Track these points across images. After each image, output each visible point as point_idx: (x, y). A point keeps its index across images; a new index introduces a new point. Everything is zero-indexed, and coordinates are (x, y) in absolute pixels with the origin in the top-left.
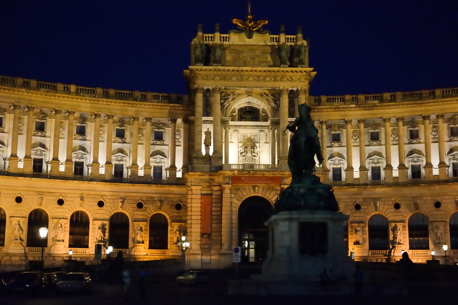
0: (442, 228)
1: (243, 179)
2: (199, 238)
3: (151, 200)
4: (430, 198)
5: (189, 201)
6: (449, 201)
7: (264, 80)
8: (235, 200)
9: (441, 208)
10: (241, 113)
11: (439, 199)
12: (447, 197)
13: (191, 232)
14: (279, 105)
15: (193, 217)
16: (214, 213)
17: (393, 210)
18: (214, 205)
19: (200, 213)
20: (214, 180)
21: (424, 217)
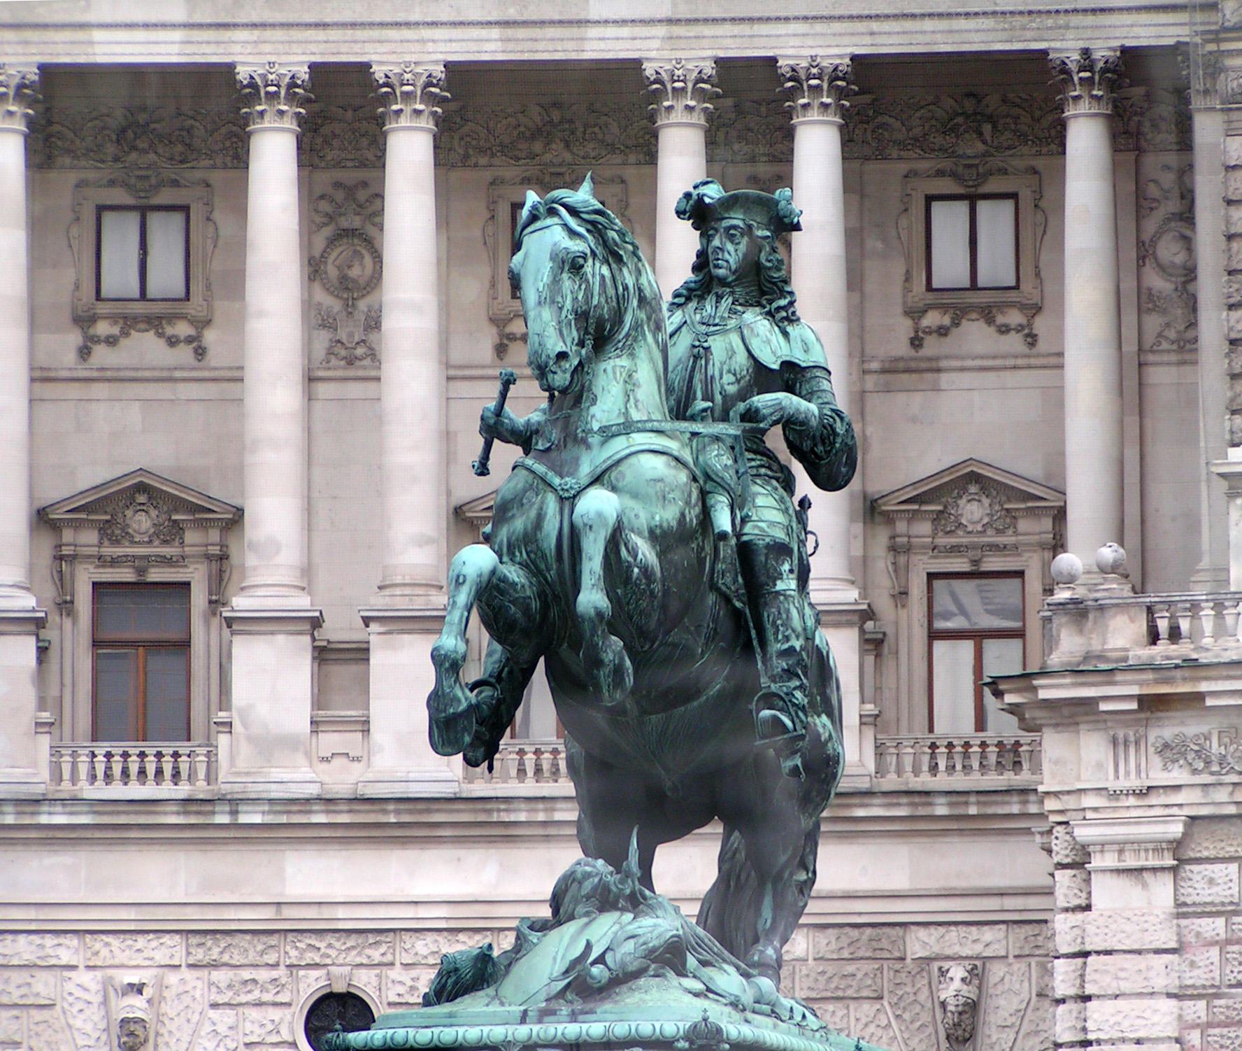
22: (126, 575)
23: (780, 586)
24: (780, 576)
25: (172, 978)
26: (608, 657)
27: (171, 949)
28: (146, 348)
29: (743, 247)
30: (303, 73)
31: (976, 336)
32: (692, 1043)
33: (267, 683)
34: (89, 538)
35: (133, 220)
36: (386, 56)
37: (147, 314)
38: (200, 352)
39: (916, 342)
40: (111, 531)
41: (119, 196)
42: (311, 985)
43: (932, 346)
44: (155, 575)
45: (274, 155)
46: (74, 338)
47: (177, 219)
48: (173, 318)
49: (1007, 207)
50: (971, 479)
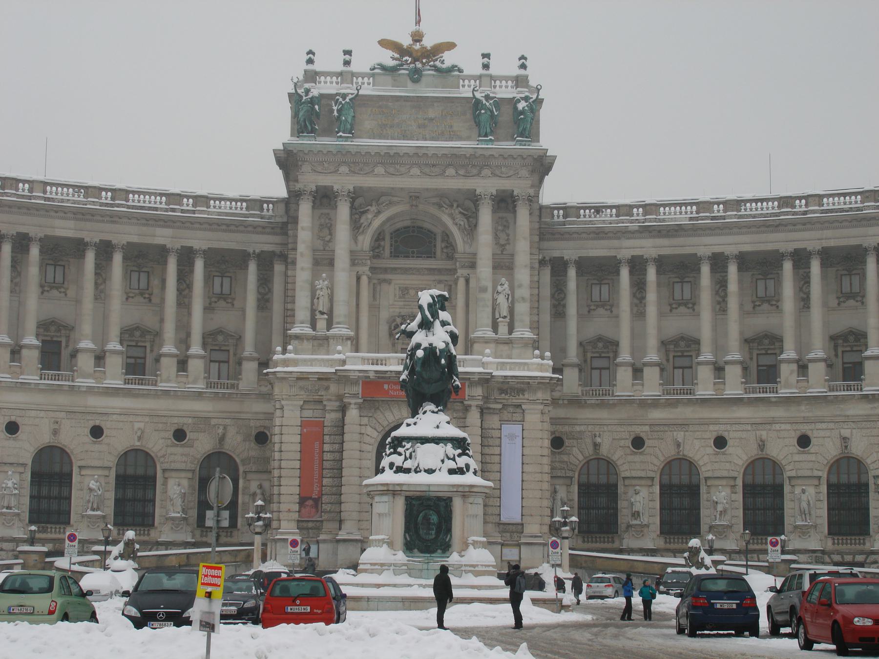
0: (811, 491)
1: (386, 387)
2: (296, 507)
3: (203, 421)
4: (788, 427)
5: (277, 430)
6: (828, 433)
7: (442, 174)
8: (369, 430)
9: (812, 448)
10: (396, 242)
11: (805, 429)
12: (824, 426)
13: (280, 494)
14: (476, 226)
15: (284, 464)
16: (327, 456)
17: (712, 449)
18: (327, 438)
19: (298, 456)
20: (327, 388)
21: (775, 466)
22: (49, 338)
25: (63, 421)
27: (63, 415)
30: (98, 241)
31: (222, 303)
35: (53, 267)
36: (116, 239)
39: (210, 304)
42: (91, 424)
43: (213, 305)
44: (55, 339)
48: (60, 287)
49: (229, 279)
50: (220, 331)
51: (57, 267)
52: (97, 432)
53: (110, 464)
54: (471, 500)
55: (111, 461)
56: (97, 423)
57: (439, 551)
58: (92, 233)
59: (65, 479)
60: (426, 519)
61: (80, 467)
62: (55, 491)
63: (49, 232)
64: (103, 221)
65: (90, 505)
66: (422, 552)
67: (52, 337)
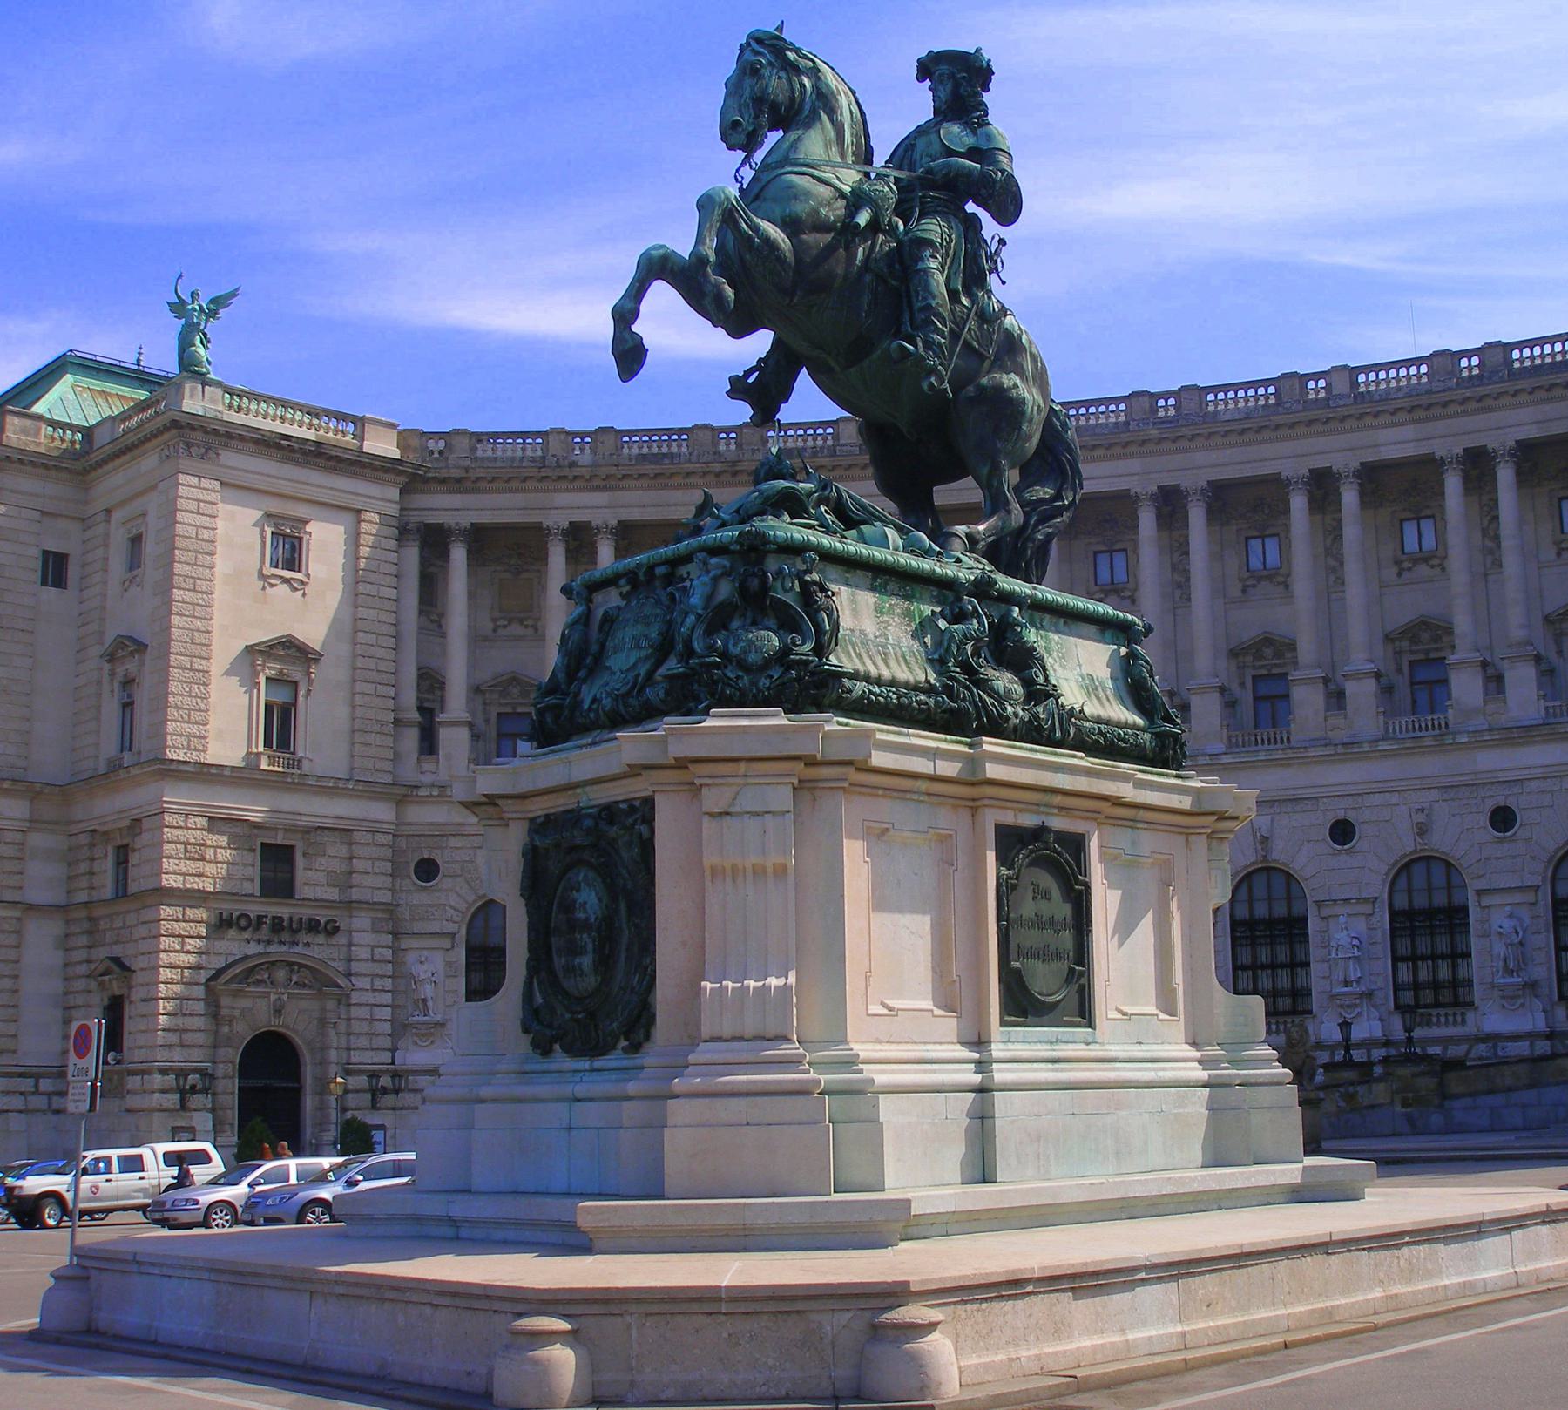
22: (1422, 656)
23: (920, 266)
24: (922, 259)
25: (1436, 806)
26: (708, 288)
28: (1423, 570)
29: (949, 86)
32: (742, 545)
33: (1466, 687)
34: (1405, 644)
36: (1492, 442)
37: (1422, 558)
38: (1443, 569)
40: (1414, 640)
41: (1408, 515)
42: (1490, 805)
44: (1432, 655)
45: (1453, 483)
46: (1395, 570)
47: (1431, 521)
51: (1422, 522)
52: (1503, 819)
53: (1537, 881)
54: (713, 799)
55: (1536, 873)
56: (1501, 801)
57: (623, 1043)
58: (1446, 438)
59: (1454, 918)
60: (568, 907)
61: (1479, 892)
62: (1443, 945)
63: (1370, 457)
64: (1465, 413)
65: (1501, 964)
66: (570, 1051)
67: (1427, 652)
